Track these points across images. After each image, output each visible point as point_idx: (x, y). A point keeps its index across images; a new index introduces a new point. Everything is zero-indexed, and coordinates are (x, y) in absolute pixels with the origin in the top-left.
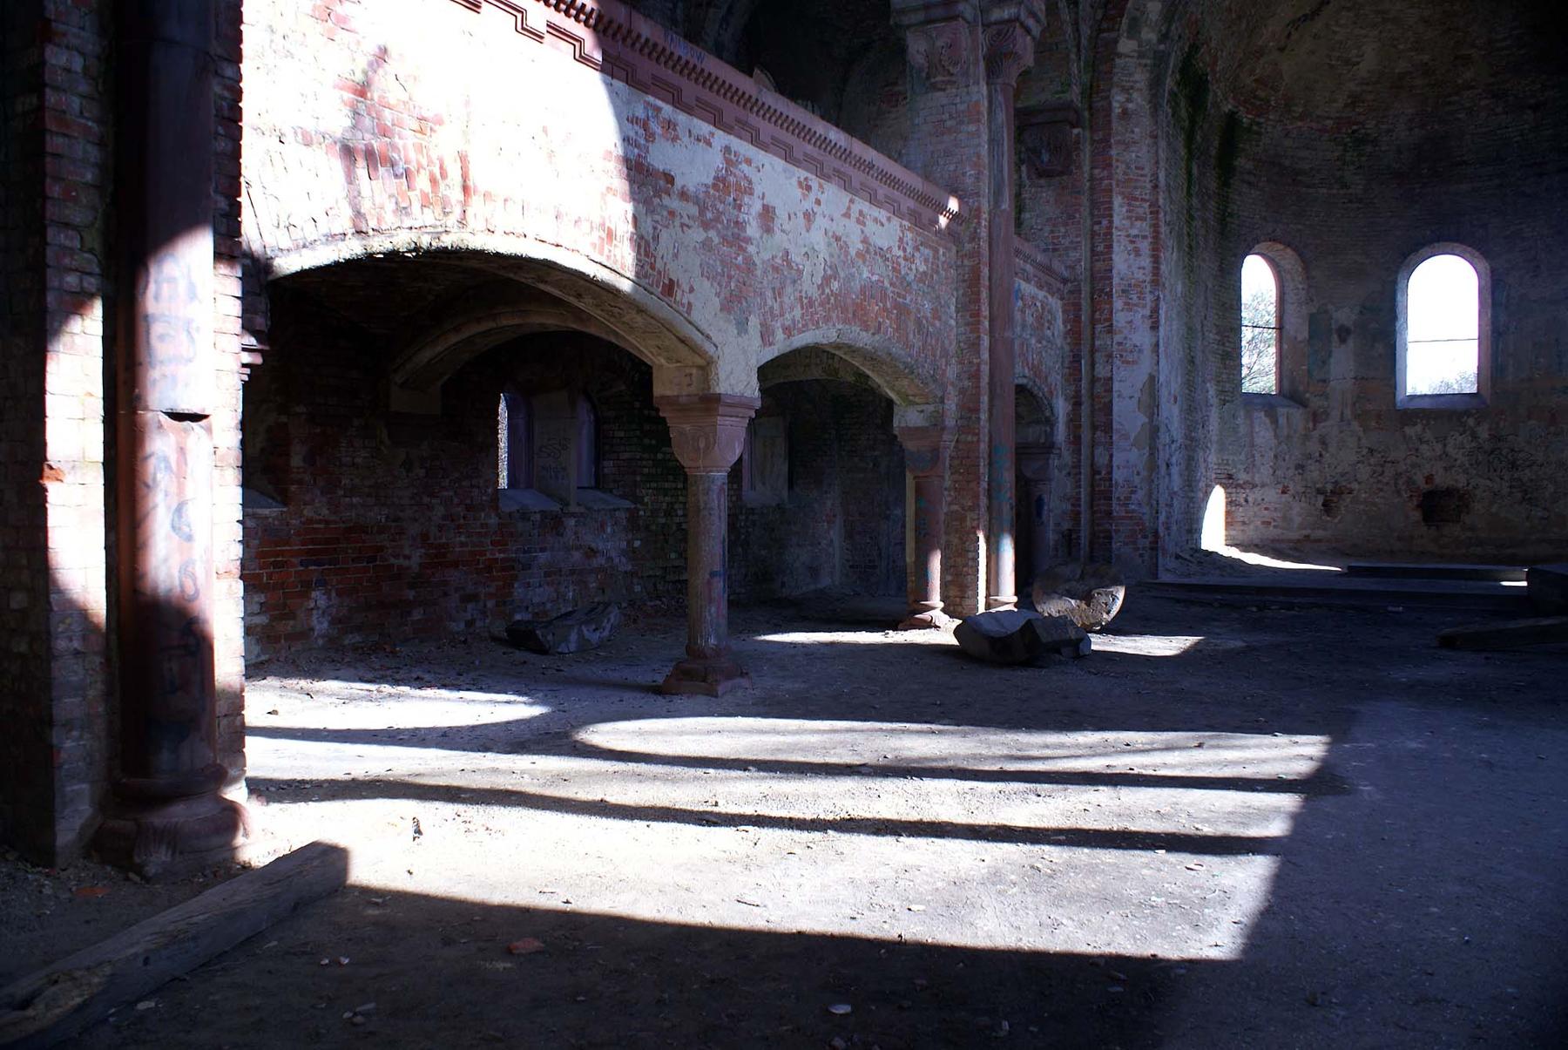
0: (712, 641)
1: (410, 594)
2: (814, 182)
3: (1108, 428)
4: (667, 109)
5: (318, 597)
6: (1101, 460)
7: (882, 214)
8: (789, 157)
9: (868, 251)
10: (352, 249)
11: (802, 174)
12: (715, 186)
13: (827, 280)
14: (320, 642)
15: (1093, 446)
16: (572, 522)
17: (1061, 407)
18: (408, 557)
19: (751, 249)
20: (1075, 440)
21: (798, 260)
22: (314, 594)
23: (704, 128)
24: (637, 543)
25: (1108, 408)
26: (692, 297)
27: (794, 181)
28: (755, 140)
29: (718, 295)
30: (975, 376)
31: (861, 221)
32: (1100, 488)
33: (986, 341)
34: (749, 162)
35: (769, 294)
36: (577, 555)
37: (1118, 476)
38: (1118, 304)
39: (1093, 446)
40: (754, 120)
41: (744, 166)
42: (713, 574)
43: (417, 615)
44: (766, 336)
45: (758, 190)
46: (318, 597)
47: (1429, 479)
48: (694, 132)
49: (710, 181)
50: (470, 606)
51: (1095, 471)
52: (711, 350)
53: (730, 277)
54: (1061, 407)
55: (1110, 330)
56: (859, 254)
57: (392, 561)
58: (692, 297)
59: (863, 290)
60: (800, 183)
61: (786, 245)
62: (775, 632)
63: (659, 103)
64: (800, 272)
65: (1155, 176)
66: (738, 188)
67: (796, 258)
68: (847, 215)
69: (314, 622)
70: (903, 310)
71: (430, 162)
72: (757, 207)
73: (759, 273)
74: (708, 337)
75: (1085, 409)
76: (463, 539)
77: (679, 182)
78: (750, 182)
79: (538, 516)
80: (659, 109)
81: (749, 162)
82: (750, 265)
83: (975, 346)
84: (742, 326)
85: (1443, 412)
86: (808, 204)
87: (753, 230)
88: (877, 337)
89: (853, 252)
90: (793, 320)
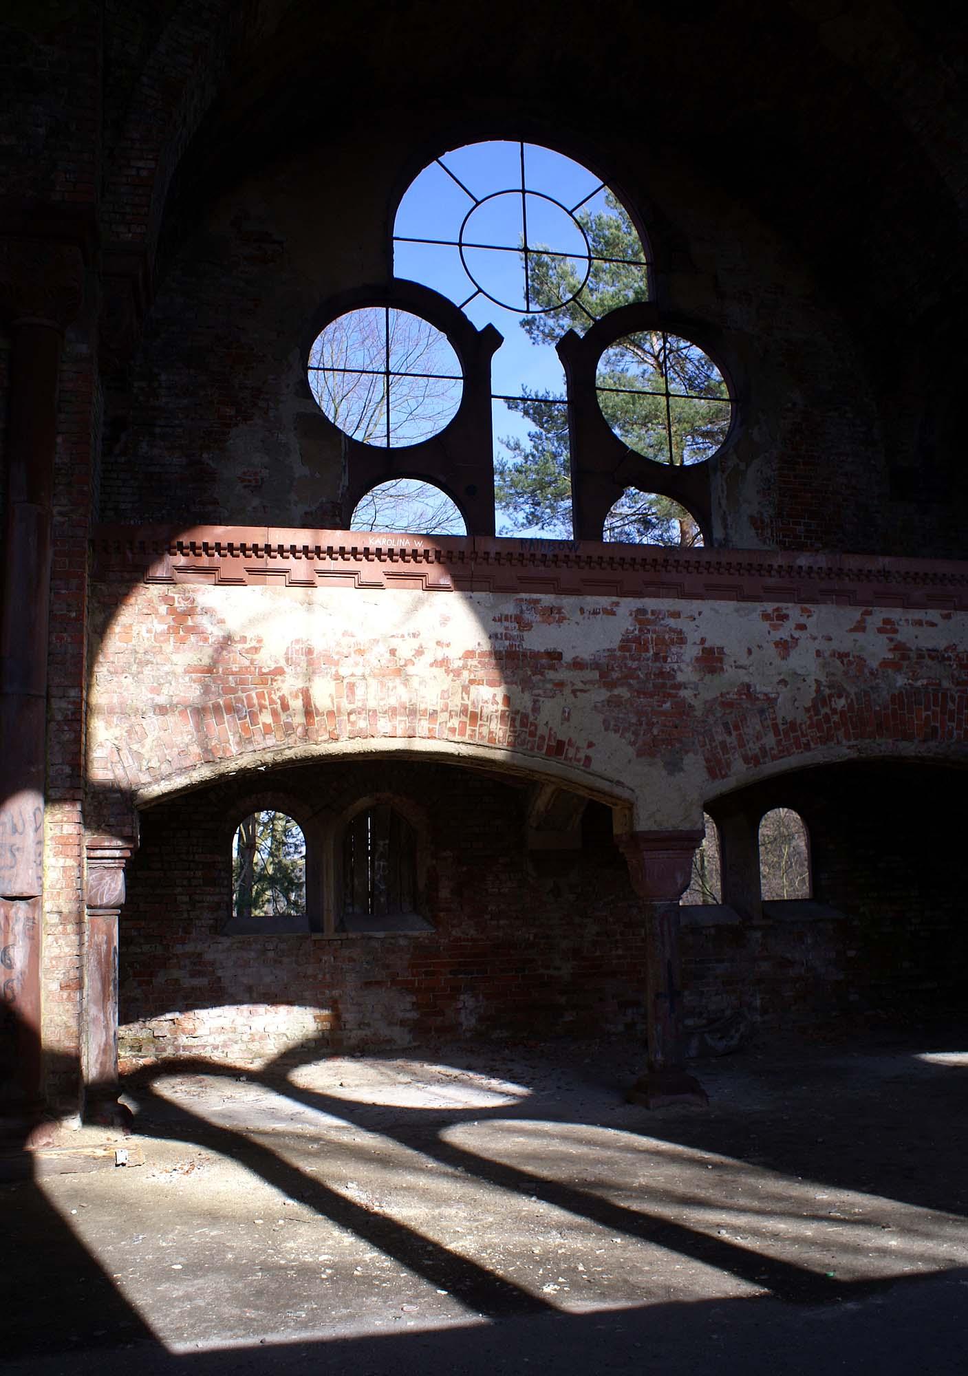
0: (659, 1057)
1: (563, 1000)
2: (793, 611)
4: (547, 599)
5: (467, 1000)
7: (933, 615)
9: (904, 657)
10: (204, 773)
11: (770, 607)
12: (622, 648)
13: (821, 700)
14: (468, 1035)
16: (758, 934)
18: (559, 969)
19: (685, 693)
21: (768, 689)
22: (462, 997)
23: (604, 601)
24: (851, 953)
26: (590, 752)
27: (756, 615)
29: (632, 744)
31: (888, 627)
34: (676, 615)
35: (720, 729)
36: (765, 966)
41: (672, 622)
42: (658, 995)
43: (569, 1017)
44: (715, 769)
45: (693, 637)
46: (467, 1000)
48: (587, 608)
49: (616, 644)
50: (629, 1011)
52: (626, 794)
53: (651, 725)
56: (885, 664)
57: (541, 971)
58: (590, 752)
59: (897, 699)
60: (766, 616)
61: (746, 679)
62: (931, 1052)
63: (535, 596)
64: (772, 701)
66: (660, 641)
67: (761, 688)
68: (860, 627)
69: (462, 1017)
71: (272, 702)
72: (691, 651)
73: (698, 713)
74: (619, 783)
76: (620, 952)
77: (568, 657)
78: (681, 632)
79: (713, 931)
80: (537, 601)
81: (676, 615)
82: (683, 709)
84: (673, 767)
86: (784, 633)
87: (687, 674)
88: (932, 744)
89: (874, 664)
90: (763, 749)
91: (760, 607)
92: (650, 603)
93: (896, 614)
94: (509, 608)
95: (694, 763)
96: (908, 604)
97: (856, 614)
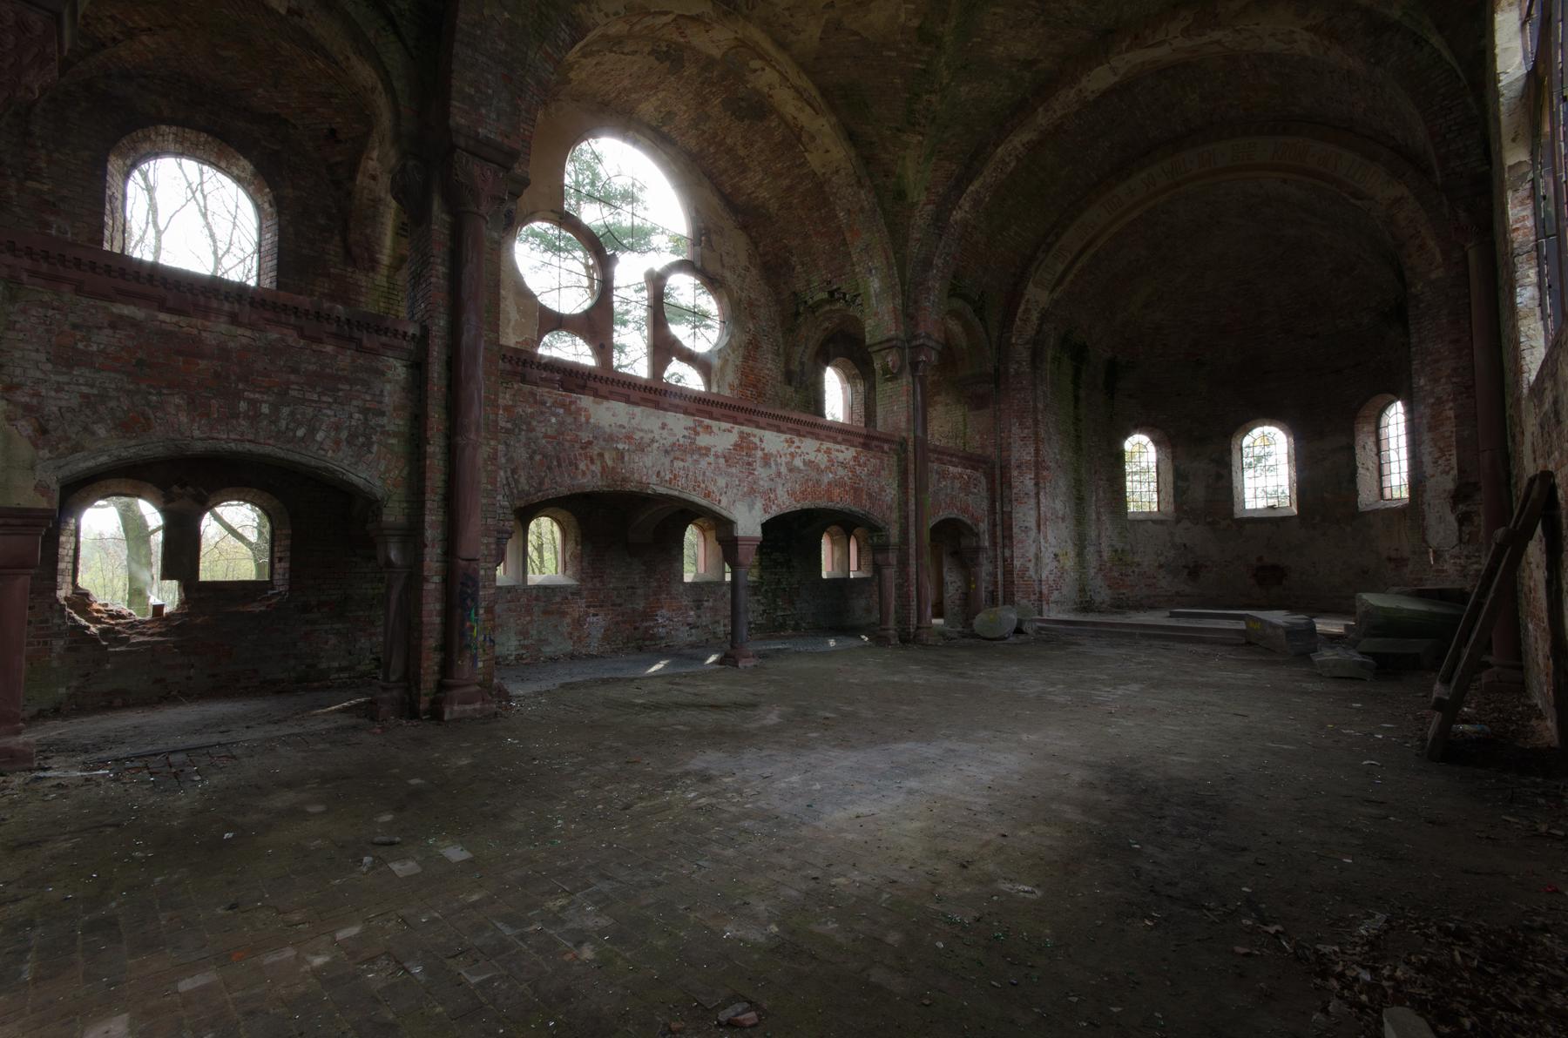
2: (796, 439)
3: (1011, 538)
4: (707, 421)
6: (1007, 554)
7: (843, 448)
8: (779, 430)
15: (1004, 546)
17: (983, 526)
20: (994, 544)
23: (728, 426)
25: (1011, 529)
28: (758, 426)
30: (906, 518)
31: (828, 451)
32: (1008, 571)
33: (912, 500)
37: (1017, 563)
38: (1015, 473)
39: (1004, 546)
40: (755, 418)
47: (1260, 559)
51: (1005, 560)
54: (983, 526)
55: (1010, 487)
65: (1035, 407)
70: (856, 490)
72: (759, 453)
75: (999, 529)
83: (906, 503)
84: (751, 507)
85: (1269, 522)
91: (784, 437)
92: (746, 429)
93: (830, 445)
94: (691, 424)
95: (759, 505)
96: (836, 442)
97: (816, 444)
